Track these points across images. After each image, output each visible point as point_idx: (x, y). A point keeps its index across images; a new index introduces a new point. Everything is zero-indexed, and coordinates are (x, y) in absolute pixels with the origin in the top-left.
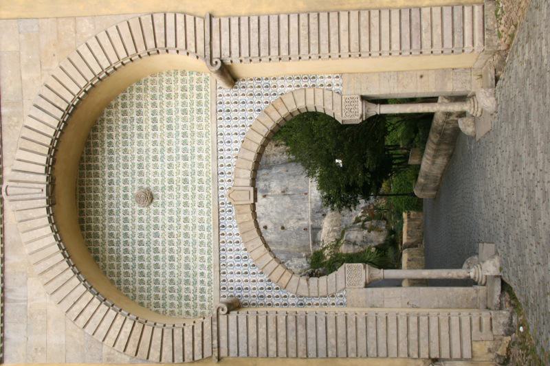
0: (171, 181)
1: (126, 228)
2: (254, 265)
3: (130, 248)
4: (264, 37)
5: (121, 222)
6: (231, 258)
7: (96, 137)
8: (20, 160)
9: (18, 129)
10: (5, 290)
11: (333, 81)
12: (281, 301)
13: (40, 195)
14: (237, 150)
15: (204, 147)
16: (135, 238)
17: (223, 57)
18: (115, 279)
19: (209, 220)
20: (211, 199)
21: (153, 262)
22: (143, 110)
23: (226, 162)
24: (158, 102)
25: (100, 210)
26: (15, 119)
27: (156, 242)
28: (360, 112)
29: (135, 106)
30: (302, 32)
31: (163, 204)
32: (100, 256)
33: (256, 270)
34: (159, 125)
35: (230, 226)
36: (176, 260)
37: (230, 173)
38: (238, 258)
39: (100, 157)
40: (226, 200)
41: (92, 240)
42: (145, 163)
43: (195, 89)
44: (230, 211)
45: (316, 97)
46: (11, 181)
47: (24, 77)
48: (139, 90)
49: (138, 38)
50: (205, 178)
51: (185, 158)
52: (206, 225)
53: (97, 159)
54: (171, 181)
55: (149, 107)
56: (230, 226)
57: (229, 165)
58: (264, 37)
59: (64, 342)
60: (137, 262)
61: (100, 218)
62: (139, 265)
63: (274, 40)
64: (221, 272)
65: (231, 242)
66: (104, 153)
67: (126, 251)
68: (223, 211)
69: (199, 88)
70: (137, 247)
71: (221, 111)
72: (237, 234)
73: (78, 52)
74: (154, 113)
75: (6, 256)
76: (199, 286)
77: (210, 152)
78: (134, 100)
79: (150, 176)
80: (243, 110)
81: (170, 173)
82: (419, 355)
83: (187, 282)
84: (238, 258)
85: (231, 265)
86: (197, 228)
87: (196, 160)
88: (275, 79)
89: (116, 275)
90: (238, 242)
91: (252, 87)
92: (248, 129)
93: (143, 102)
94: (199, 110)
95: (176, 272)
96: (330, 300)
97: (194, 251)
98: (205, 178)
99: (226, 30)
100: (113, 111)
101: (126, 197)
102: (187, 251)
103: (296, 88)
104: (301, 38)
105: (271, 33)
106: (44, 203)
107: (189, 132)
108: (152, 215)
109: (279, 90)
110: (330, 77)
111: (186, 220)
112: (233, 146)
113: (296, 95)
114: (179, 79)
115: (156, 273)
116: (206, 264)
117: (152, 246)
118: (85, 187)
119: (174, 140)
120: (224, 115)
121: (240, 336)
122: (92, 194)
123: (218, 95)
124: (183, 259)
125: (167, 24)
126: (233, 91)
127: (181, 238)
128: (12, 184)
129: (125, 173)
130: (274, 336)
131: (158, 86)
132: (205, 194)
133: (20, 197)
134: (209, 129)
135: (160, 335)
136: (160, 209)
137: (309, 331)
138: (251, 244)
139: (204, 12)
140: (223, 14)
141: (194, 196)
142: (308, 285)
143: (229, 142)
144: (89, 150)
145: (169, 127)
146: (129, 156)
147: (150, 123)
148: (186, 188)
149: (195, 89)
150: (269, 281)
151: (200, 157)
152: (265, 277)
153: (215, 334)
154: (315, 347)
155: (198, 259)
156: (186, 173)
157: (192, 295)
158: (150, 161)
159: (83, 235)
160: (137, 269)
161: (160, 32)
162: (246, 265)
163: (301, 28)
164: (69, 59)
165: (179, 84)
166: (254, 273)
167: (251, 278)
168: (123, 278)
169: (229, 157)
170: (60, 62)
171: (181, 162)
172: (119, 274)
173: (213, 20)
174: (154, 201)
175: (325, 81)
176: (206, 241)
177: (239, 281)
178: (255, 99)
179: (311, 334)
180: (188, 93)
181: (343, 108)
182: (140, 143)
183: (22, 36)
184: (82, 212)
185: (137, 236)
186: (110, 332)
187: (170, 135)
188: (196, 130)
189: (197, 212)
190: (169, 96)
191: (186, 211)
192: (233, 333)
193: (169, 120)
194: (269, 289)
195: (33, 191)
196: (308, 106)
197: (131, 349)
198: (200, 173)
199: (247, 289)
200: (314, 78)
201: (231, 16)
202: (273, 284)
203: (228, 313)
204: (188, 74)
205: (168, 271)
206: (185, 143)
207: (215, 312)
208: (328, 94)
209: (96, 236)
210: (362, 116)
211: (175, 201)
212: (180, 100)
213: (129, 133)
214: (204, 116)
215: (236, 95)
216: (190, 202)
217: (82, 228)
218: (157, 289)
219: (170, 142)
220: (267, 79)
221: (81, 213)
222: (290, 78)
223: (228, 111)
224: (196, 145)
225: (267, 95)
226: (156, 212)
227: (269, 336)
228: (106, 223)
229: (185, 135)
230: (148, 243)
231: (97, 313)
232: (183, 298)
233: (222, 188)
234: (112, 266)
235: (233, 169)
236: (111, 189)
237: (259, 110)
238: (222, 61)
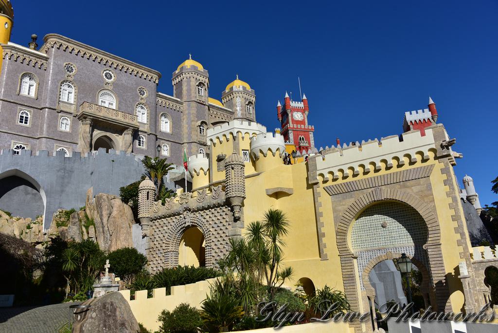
0: (391, 232)
12: (360, 270)
19: (381, 245)
23: (400, 250)
34: (409, 226)
49: (431, 222)
54: (391, 232)
70: (370, 224)
74: (413, 224)
81: (394, 232)
96: (362, 285)
102: (371, 240)
106: (376, 200)
111: (380, 239)
115: (363, 231)
132: (389, 244)
180: (421, 235)
197: (339, 230)
209: (371, 211)
217: (373, 206)
230: (371, 227)
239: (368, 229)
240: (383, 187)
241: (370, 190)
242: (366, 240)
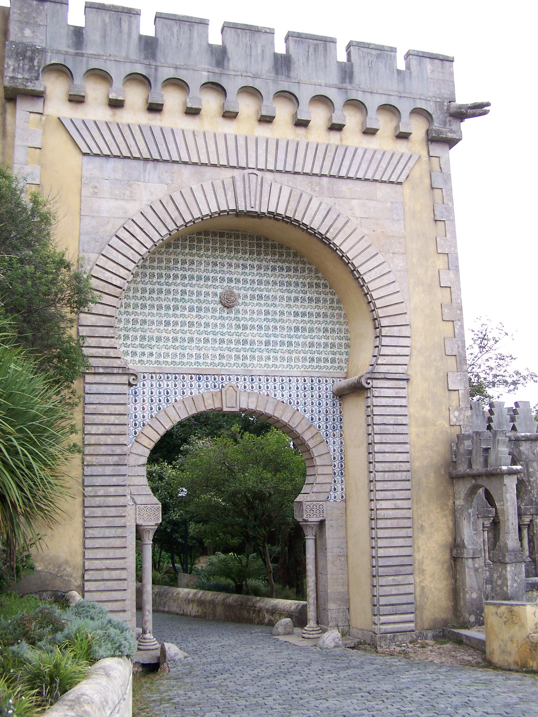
0: (245, 327)
1: (199, 278)
2: (160, 409)
3: (179, 281)
4: (391, 429)
5: (205, 274)
6: (168, 385)
7: (288, 255)
8: (281, 189)
9: (309, 191)
10: (156, 162)
11: (339, 493)
13: (248, 205)
14: (275, 395)
15: (278, 363)
16: (188, 287)
17: (374, 390)
18: (147, 263)
20: (227, 367)
21: (164, 303)
22: (314, 304)
23: (263, 384)
24: (321, 319)
25: (217, 253)
26: (317, 189)
27: (185, 308)
28: (310, 520)
29: (318, 296)
30: (395, 464)
31: (221, 318)
32: (171, 250)
34: (299, 318)
35: (199, 386)
36: (166, 328)
37: (252, 387)
38: (168, 393)
39: (269, 257)
42: (262, 302)
43: (333, 356)
44: (215, 386)
45: (325, 476)
46: (262, 179)
48: (332, 301)
50: (248, 362)
51: (267, 343)
52: (201, 361)
53: (267, 254)
54: (245, 327)
55: (316, 310)
56: (199, 386)
57: (260, 387)
58: (391, 429)
59: (103, 215)
60: (164, 287)
61: (209, 253)
62: (162, 289)
63: (388, 439)
64: (153, 375)
65: (183, 386)
66: (273, 262)
67: (176, 277)
68: (215, 379)
69: (333, 361)
70: (180, 288)
71: (312, 381)
72: (191, 393)
73: (377, 254)
74: (311, 314)
75: (188, 166)
76: (139, 350)
77: (273, 369)
78: (323, 296)
79: (250, 306)
80: (312, 403)
81: (252, 327)
82: (88, 581)
83: (143, 338)
84: (168, 393)
85: (160, 385)
86: (198, 352)
87: (265, 354)
88: (341, 435)
89: (151, 264)
90: (183, 393)
91: (334, 412)
93: (320, 304)
94: (312, 360)
95: (154, 327)
97: (174, 347)
98: (248, 362)
99: (396, 393)
100: (313, 275)
101: (230, 280)
102: (175, 339)
103: (332, 456)
104: (389, 464)
105: (394, 436)
106: (242, 208)
107: (292, 348)
108: (212, 306)
109: (331, 440)
110: (342, 489)
111: (207, 341)
112: (279, 393)
113: (325, 456)
114: (341, 341)
115: (153, 306)
116: (161, 359)
117: (180, 304)
119: (285, 333)
120: (308, 385)
121: (107, 396)
123: (327, 379)
124: (167, 335)
125: (402, 339)
126: (329, 393)
127: (188, 334)
128: (259, 180)
129: (253, 282)
130: (107, 432)
131: (335, 320)
132: (232, 362)
133: (247, 186)
134: (295, 369)
135: (108, 314)
136: (217, 315)
137: (112, 468)
138: (182, 406)
140: (410, 390)
141: (230, 350)
142: (139, 466)
143: (283, 388)
144: (275, 248)
145: (297, 329)
146: (270, 287)
147: (301, 310)
148: (238, 342)
149: (333, 356)
150: (144, 425)
151: (269, 358)
152: (148, 420)
153: (109, 371)
154: (95, 474)
155: (166, 351)
156: (252, 343)
157: (129, 342)
158: (265, 308)
159: (193, 234)
160: (157, 287)
162: (160, 401)
163: (398, 464)
164: (371, 245)
165: (337, 341)
166: (151, 409)
167: (147, 406)
168: (148, 271)
169: (268, 387)
170: (368, 235)
171: (264, 339)
172: (153, 268)
173: (406, 382)
174: (225, 309)
175: (339, 485)
176: (185, 360)
177: (144, 393)
179: (108, 470)
180: (329, 349)
181: (315, 503)
182: (282, 298)
183: (389, 204)
184: (216, 235)
185: (191, 289)
186: (112, 263)
187: (290, 329)
188: (294, 355)
189: (214, 353)
190: (326, 330)
191: (215, 341)
192: (110, 389)
193: (304, 329)
194: (135, 425)
195: (253, 199)
196: (316, 468)
198: (253, 358)
199: (136, 401)
200: (342, 474)
201: (408, 399)
202: (140, 429)
204: (346, 350)
205: (155, 319)
206: (282, 343)
207: (132, 372)
208: (327, 488)
209: (191, 247)
210: (306, 521)
211: (225, 330)
212: (323, 340)
213: (292, 288)
214: (307, 364)
215: (327, 397)
216: (225, 346)
217: (199, 233)
218: (136, 306)
219: (283, 328)
220: (341, 427)
221: (214, 234)
222: (341, 451)
223: (312, 389)
224: (279, 355)
225: (327, 427)
226: (214, 310)
227: (107, 427)
228: (204, 258)
229: (290, 344)
231: (132, 250)
232: (126, 333)
233: (237, 379)
234: (160, 261)
235: (256, 391)
236: (238, 266)
237: (312, 419)
238: (370, 388)
239: (172, 304)
240: (269, 176)
241: (227, 174)
242: (159, 339)
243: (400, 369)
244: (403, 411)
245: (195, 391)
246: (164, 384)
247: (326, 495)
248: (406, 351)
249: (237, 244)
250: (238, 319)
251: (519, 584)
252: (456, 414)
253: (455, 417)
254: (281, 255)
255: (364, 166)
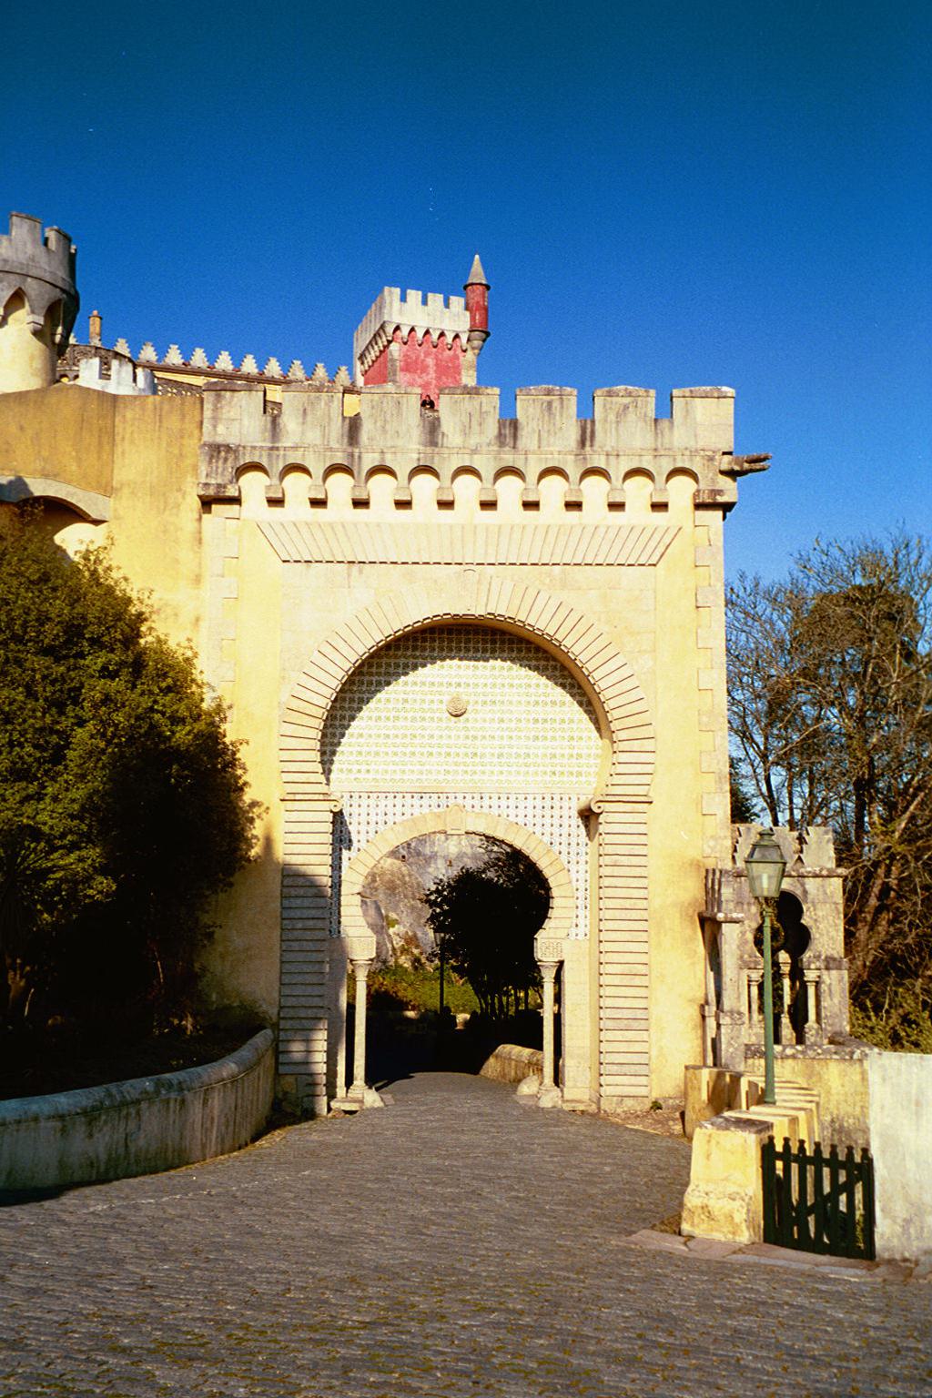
4: (624, 860)
7: (529, 650)
18: (365, 669)
26: (547, 581)
28: (544, 959)
32: (391, 653)
33: (372, 834)
34: (539, 725)
40: (451, 801)
41: (410, 643)
47: (592, 592)
51: (501, 755)
52: (424, 777)
58: (624, 860)
82: (283, 1018)
92: (531, 829)
98: (476, 777)
109: (573, 867)
118: (471, 636)
122: (463, 645)
126: (575, 813)
132: (459, 777)
139: (653, 796)
144: (513, 643)
161: (636, 745)
168: (366, 678)
171: (497, 751)
172: (371, 674)
178: (564, 839)
197: (295, 704)
203: (332, 812)
209: (415, 648)
224: (515, 768)
234: (379, 666)
243: (642, 790)
244: (643, 839)
245: (417, 811)
246: (383, 802)
247: (566, 931)
248: (648, 769)
249: (467, 641)
250: (466, 729)
251: (736, 1049)
252: (712, 843)
253: (709, 847)
254: (520, 650)
255: (605, 548)
